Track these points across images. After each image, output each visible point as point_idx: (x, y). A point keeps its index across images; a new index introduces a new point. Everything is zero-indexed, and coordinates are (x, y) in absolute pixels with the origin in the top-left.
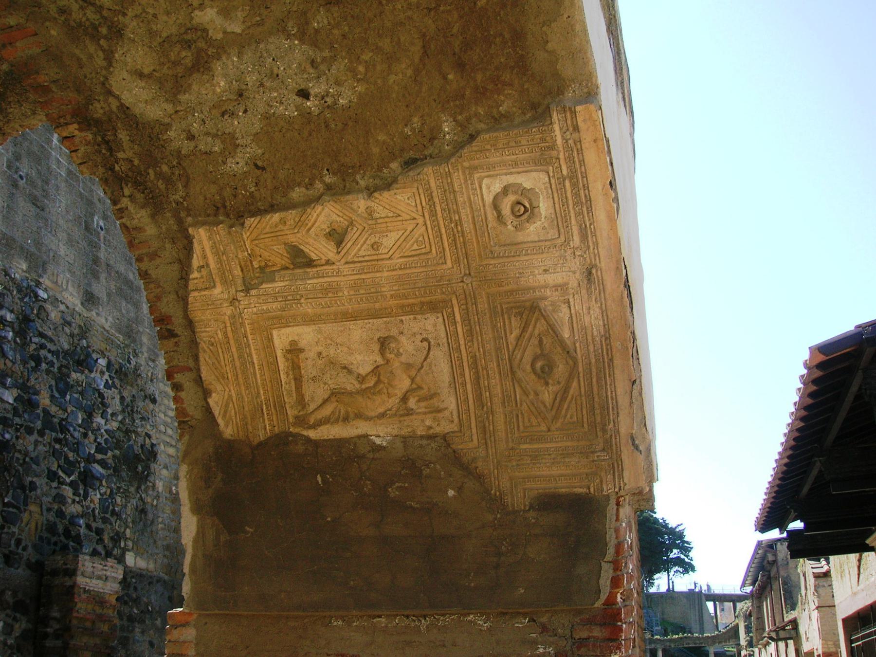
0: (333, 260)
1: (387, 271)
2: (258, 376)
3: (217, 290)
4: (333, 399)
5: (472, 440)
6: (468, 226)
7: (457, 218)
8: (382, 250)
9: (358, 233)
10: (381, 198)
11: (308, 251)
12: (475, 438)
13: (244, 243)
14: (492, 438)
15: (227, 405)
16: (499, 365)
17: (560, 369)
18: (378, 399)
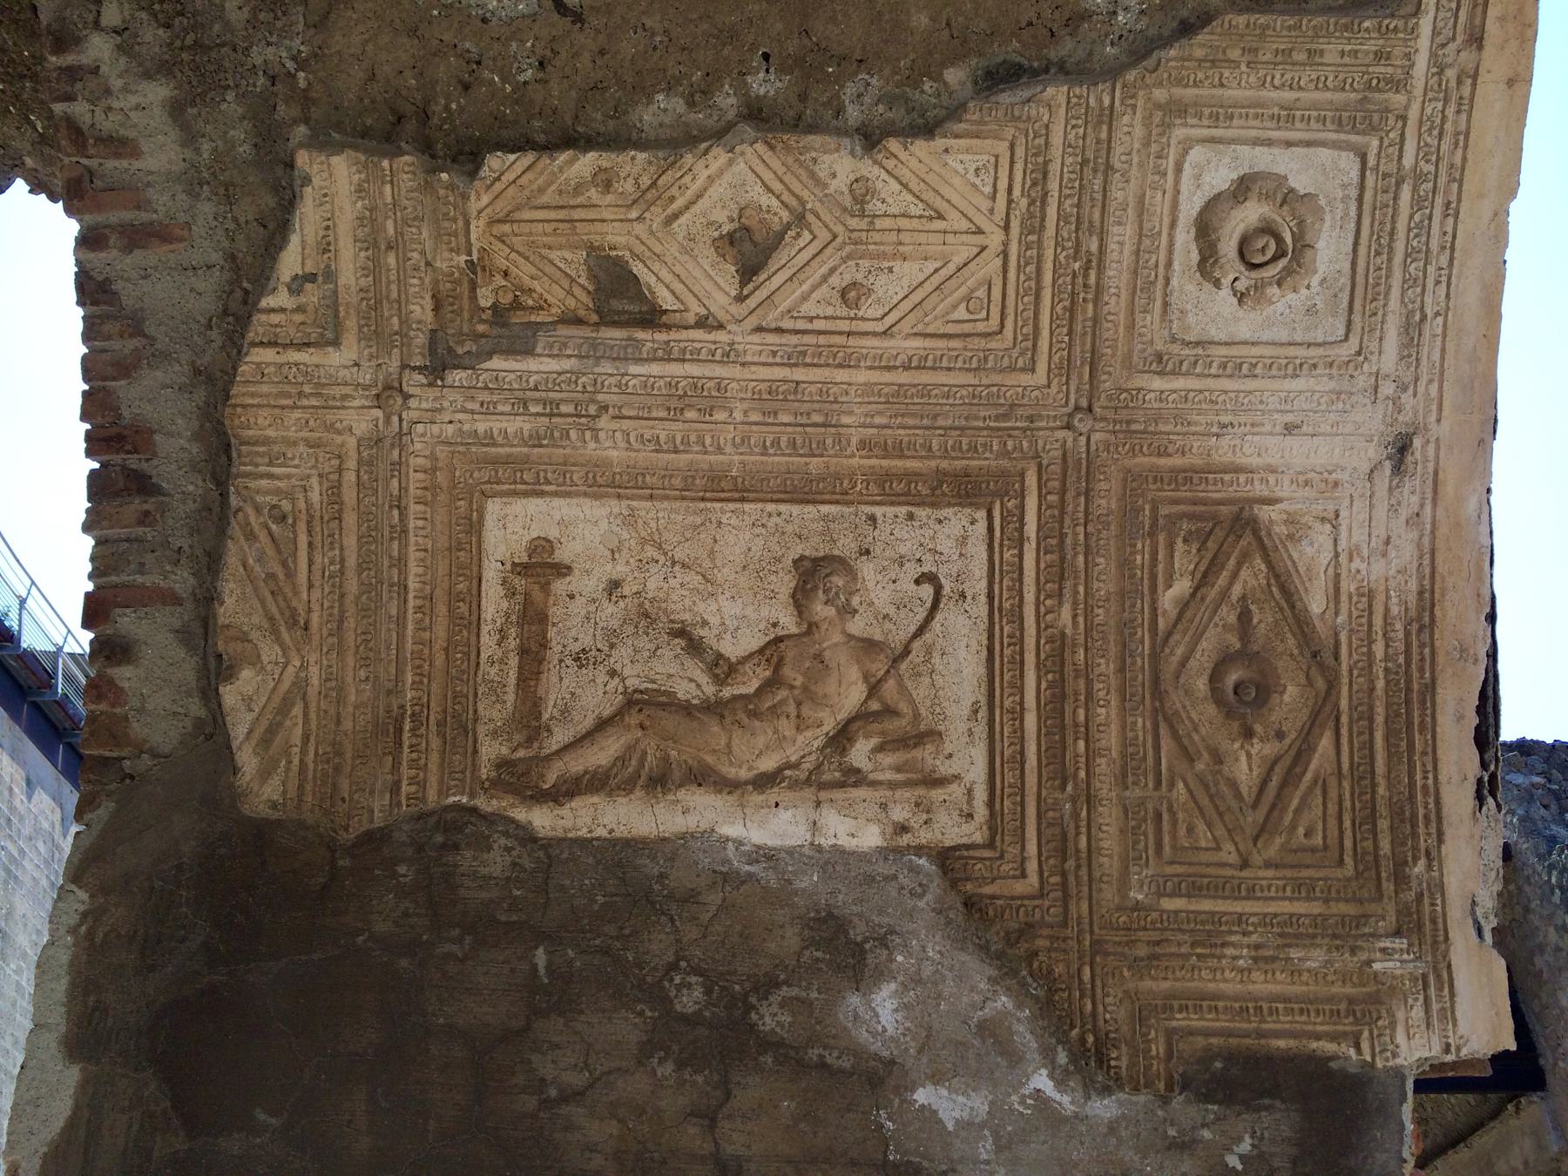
0: (722, 316)
1: (870, 368)
2: (410, 627)
3: (336, 359)
4: (633, 719)
5: (1024, 875)
6: (1117, 275)
7: (1094, 247)
8: (869, 310)
9: (812, 250)
10: (903, 155)
11: (652, 280)
12: (1032, 866)
13: (467, 224)
14: (1084, 872)
15: (284, 708)
16: (1122, 670)
17: (1286, 698)
18: (764, 734)
